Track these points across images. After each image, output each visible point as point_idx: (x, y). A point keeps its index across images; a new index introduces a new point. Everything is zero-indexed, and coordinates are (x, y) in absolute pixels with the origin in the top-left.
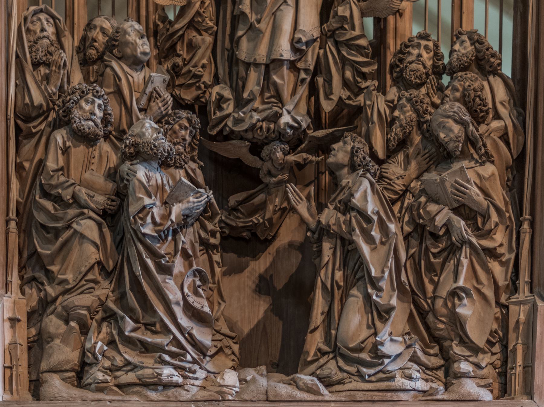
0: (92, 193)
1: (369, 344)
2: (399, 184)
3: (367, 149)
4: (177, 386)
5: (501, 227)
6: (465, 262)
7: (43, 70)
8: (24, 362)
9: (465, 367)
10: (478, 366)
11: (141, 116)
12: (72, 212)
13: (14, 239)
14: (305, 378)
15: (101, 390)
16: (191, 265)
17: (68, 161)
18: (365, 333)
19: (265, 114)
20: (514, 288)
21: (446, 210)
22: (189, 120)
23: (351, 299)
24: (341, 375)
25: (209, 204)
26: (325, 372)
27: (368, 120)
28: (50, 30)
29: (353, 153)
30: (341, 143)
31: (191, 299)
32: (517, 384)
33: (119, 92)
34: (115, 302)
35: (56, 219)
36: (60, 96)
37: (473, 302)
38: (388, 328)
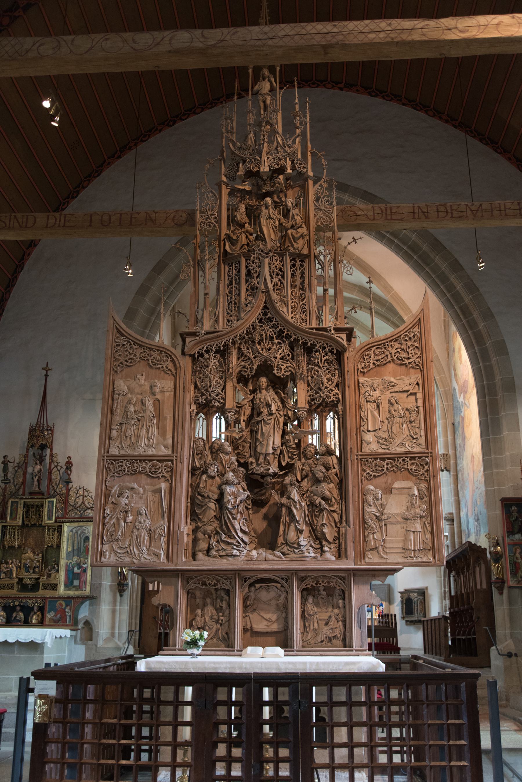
0: (213, 494)
1: (297, 541)
2: (305, 490)
3: (295, 479)
4: (238, 556)
5: (336, 503)
6: (325, 514)
7: (199, 455)
8: (191, 548)
9: (326, 549)
10: (330, 548)
11: (228, 469)
12: (207, 500)
13: (189, 508)
14: (277, 553)
15: (214, 557)
16: (242, 516)
17: (206, 484)
18: (296, 538)
19: (265, 468)
20: (341, 522)
21: (319, 498)
22: (243, 471)
23: (291, 527)
24: (288, 552)
25: (248, 496)
26: (283, 551)
27: (296, 469)
28: (202, 443)
29: (291, 481)
30: (287, 477)
31: (243, 527)
32: (343, 554)
33: (222, 463)
34: (219, 528)
35: (202, 502)
36: (205, 464)
37: (328, 527)
38: (303, 536)
